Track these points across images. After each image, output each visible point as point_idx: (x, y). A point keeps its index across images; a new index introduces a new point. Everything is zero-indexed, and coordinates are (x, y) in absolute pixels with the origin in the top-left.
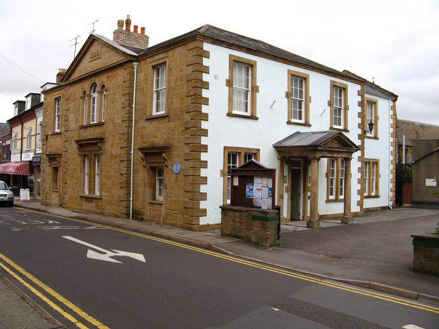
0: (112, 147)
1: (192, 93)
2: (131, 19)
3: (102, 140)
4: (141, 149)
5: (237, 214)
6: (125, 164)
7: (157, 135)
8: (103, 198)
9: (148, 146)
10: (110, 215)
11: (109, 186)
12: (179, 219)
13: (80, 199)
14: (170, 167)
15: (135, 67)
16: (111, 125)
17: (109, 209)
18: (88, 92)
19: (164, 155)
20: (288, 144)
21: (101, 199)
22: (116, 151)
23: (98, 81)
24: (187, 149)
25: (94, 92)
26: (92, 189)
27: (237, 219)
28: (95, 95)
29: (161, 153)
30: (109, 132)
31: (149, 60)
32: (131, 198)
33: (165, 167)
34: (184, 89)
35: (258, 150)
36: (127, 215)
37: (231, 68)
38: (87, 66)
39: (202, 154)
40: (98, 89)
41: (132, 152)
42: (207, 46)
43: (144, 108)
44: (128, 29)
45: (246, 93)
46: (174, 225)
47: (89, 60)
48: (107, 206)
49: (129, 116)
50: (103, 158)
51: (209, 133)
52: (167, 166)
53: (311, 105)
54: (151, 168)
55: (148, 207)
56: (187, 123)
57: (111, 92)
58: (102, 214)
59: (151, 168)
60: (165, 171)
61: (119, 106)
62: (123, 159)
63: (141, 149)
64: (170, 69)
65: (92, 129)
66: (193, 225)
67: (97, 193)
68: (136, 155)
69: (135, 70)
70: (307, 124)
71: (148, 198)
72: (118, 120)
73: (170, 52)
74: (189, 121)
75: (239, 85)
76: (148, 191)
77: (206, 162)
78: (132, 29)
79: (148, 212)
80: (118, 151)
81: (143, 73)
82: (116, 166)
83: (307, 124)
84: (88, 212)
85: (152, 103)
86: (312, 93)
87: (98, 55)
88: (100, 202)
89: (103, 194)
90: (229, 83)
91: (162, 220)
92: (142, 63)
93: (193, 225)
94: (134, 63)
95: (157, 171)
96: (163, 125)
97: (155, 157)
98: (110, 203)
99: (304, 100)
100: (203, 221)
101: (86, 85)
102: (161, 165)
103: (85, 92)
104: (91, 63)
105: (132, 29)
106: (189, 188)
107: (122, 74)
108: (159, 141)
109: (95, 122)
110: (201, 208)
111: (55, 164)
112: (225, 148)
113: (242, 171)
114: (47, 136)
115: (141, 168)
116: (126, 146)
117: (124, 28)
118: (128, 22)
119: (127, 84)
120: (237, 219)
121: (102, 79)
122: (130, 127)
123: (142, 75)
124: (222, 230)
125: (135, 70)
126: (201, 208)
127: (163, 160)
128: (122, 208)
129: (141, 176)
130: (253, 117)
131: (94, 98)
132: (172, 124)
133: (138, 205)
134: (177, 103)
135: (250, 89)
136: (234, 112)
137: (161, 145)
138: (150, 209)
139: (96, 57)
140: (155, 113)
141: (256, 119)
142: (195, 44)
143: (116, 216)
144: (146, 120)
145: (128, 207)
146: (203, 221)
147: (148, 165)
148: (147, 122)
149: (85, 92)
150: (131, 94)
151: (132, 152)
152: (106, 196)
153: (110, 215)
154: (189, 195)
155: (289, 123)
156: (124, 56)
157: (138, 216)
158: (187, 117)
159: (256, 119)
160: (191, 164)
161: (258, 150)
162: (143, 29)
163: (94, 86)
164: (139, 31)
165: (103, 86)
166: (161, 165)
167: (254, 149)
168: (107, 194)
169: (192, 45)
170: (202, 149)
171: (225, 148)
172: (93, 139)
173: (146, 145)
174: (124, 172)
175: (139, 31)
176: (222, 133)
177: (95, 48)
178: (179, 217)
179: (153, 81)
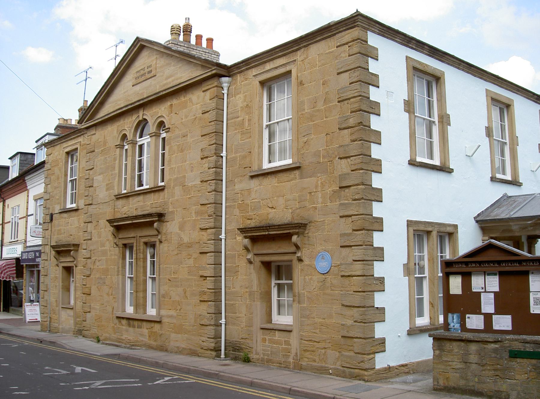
0: (181, 228)
1: (352, 122)
2: (191, 23)
3: (161, 216)
4: (243, 230)
5: (473, 347)
6: (210, 258)
7: (276, 205)
8: (165, 320)
9: (258, 224)
10: (180, 351)
11: (177, 298)
12: (332, 358)
13: (116, 321)
14: (306, 261)
15: (225, 85)
16: (178, 191)
17: (177, 340)
18: (130, 137)
19: (294, 238)
20: (503, 214)
21: (160, 322)
22: (191, 235)
23: (151, 115)
24: (346, 226)
25: (141, 137)
27: (473, 358)
28: (145, 140)
29: (288, 237)
30: (171, 201)
31: (254, 71)
32: (223, 321)
33: (295, 262)
34: (335, 117)
35: (456, 226)
36: (217, 350)
37: (410, 80)
38: (127, 93)
39: (376, 235)
40: (151, 127)
41: (223, 236)
42: (374, 40)
43: (244, 157)
44: (187, 40)
45: (430, 124)
46: (322, 371)
47: (131, 84)
48: (173, 335)
49: (216, 172)
50: (162, 249)
51: (385, 195)
52: (300, 260)
53: (520, 150)
54: (263, 263)
55: (260, 335)
56: (342, 177)
57: (177, 132)
58: (162, 348)
59: (263, 263)
60: (297, 270)
61: (194, 155)
62: (206, 250)
63: (243, 230)
64: (301, 83)
65: (141, 198)
66: (366, 370)
67: (152, 312)
68: (232, 243)
69: (225, 92)
70: (515, 183)
71: (258, 321)
72: (193, 180)
73: (299, 53)
74: (348, 174)
75: (421, 112)
76: (258, 307)
77: (382, 249)
78: (193, 41)
79: (259, 346)
80: (196, 235)
81: (241, 96)
82: (191, 262)
83: (515, 183)
84: (132, 346)
85: (261, 146)
86: (520, 130)
87: (150, 72)
88: (157, 326)
89: (163, 312)
90: (409, 106)
91: (291, 360)
92: (239, 78)
93: (366, 370)
94: (224, 79)
95: (277, 271)
96: (288, 185)
97: (273, 245)
98: (179, 329)
99: (507, 141)
100: (381, 361)
101: (128, 125)
102: (286, 258)
103: (124, 137)
104: (138, 88)
105: (193, 41)
106: (356, 300)
107: (199, 99)
108: (281, 214)
109: (145, 187)
110: (376, 337)
111: (66, 261)
112: (410, 223)
113: (467, 263)
114: (52, 215)
115: (243, 263)
116: (212, 225)
117: (181, 38)
118: (187, 30)
119: (211, 116)
120: (473, 358)
121: (161, 111)
122: (218, 191)
123: (239, 100)
124: (436, 379)
125: (225, 92)
126: (376, 337)
127: (293, 249)
128: (204, 339)
129: (242, 277)
130: (444, 169)
131: (141, 147)
132: (309, 182)
133: (237, 333)
134: (318, 143)
135: (436, 119)
136: (419, 159)
137: (286, 222)
138: (264, 340)
139: (148, 75)
140: (266, 166)
141: (450, 171)
142: (355, 33)
143: (193, 353)
144: (252, 177)
145: (217, 337)
146: (381, 361)
147: (258, 259)
148: (256, 181)
149: (124, 137)
150: (219, 133)
151: (223, 236)
152: (171, 316)
153: (180, 351)
154: (355, 313)
155: (493, 179)
156: (203, 66)
157: (238, 353)
158: (344, 166)
159: (450, 171)
160: (358, 253)
161: (456, 226)
162: (210, 41)
163: (142, 125)
164: (204, 44)
165: (161, 124)
166: (286, 258)
167: (450, 225)
168: (172, 313)
169: (348, 36)
170: (376, 226)
171: (410, 223)
172: (144, 216)
173: (252, 224)
174: (209, 272)
175: (204, 44)
176: (405, 196)
177: (144, 60)
178: (332, 354)
179: (262, 107)
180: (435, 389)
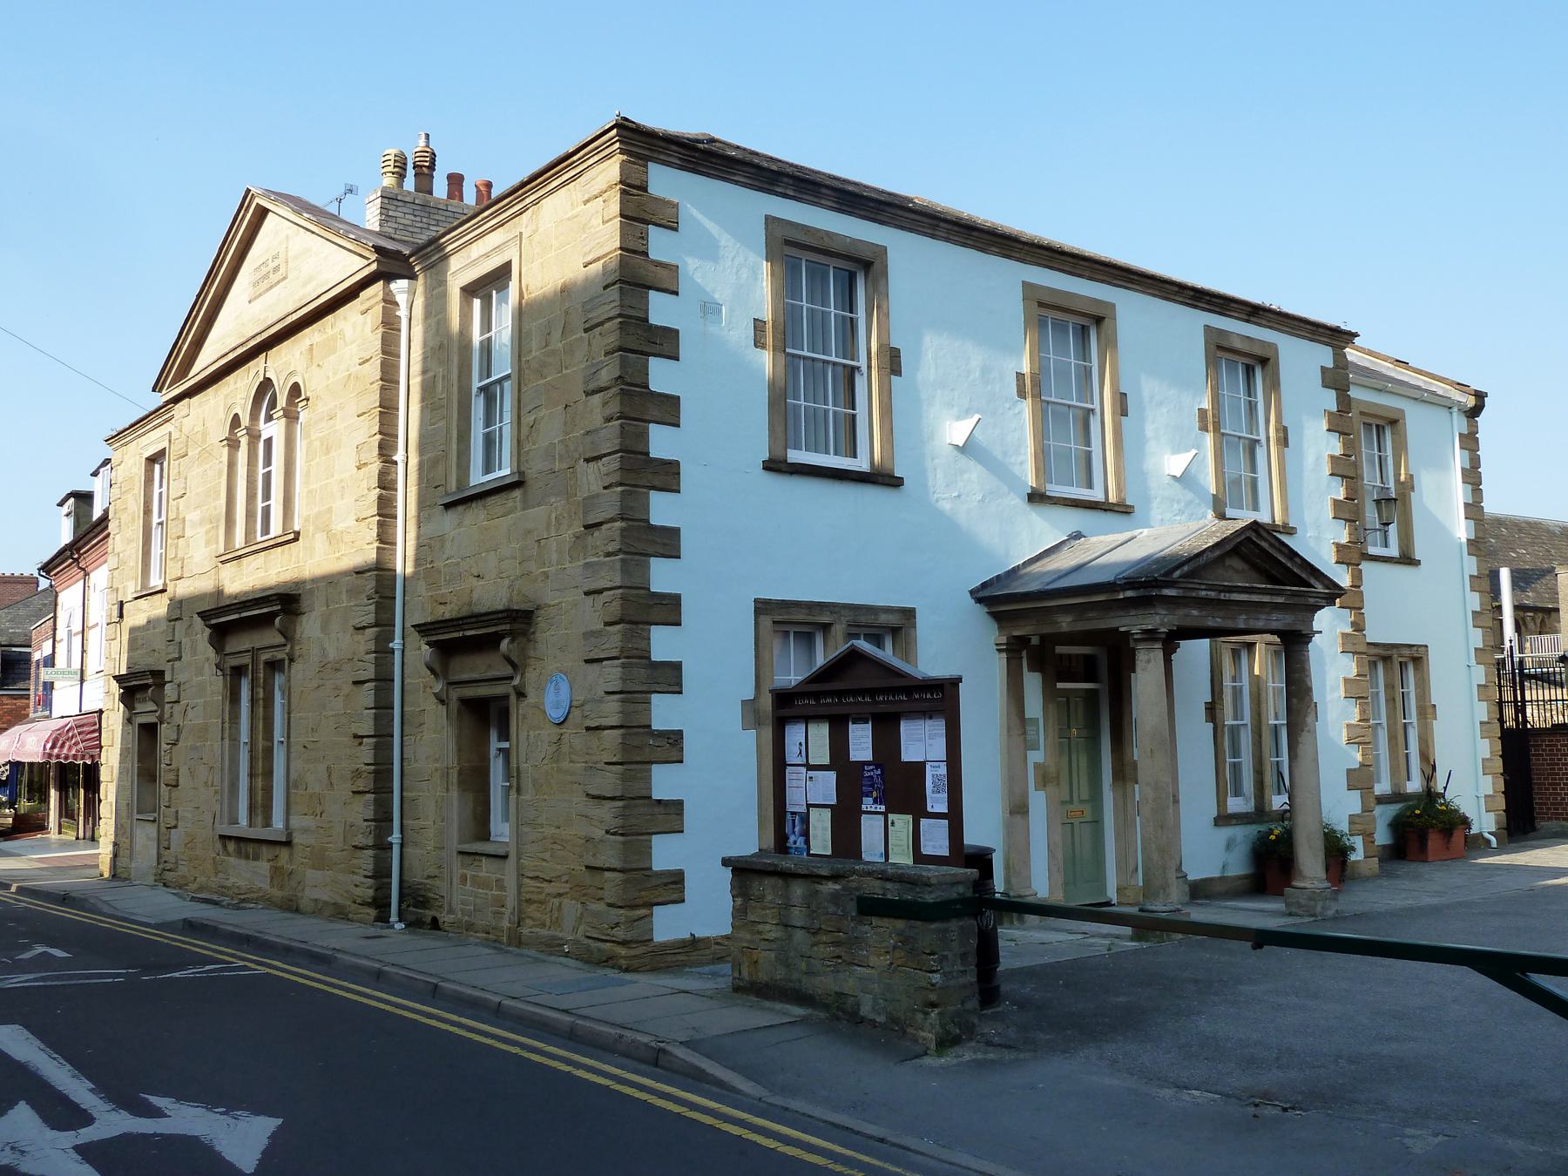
0: (325, 628)
4: (423, 629)
5: (798, 890)
6: (367, 695)
8: (298, 839)
9: (454, 615)
12: (571, 920)
13: (219, 845)
14: (532, 698)
17: (318, 886)
18: (245, 420)
25: (269, 418)
26: (261, 807)
27: (798, 916)
33: (513, 698)
35: (909, 614)
36: (380, 904)
41: (396, 644)
50: (300, 673)
54: (466, 703)
56: (590, 502)
58: (291, 906)
68: (412, 657)
74: (597, 496)
76: (455, 804)
77: (677, 667)
78: (440, 189)
79: (460, 893)
84: (241, 902)
87: (276, 269)
88: (284, 853)
98: (320, 861)
100: (668, 925)
102: (498, 690)
105: (440, 189)
111: (147, 710)
114: (121, 604)
120: (798, 916)
127: (509, 670)
131: (269, 442)
132: (538, 513)
137: (501, 607)
139: (273, 277)
140: (478, 478)
143: (340, 913)
145: (381, 874)
146: (668, 925)
147: (455, 694)
148: (452, 517)
157: (420, 909)
161: (909, 614)
165: (295, 390)
168: (308, 822)
174: (367, 727)
178: (571, 908)
180: (736, 989)
